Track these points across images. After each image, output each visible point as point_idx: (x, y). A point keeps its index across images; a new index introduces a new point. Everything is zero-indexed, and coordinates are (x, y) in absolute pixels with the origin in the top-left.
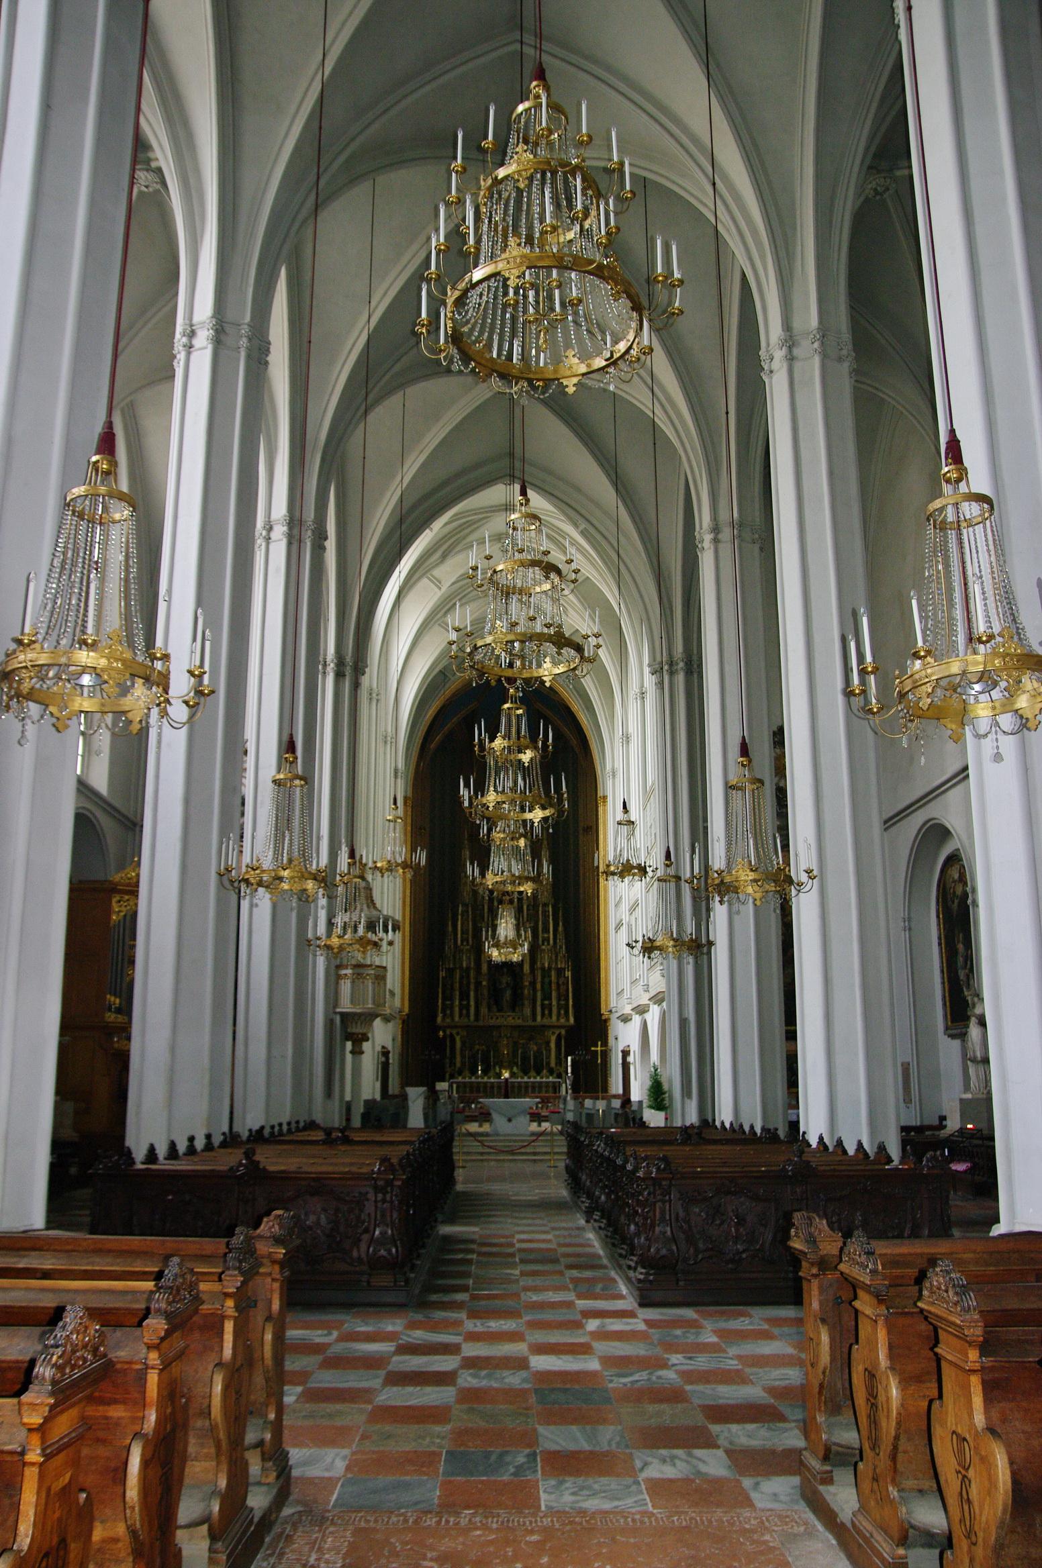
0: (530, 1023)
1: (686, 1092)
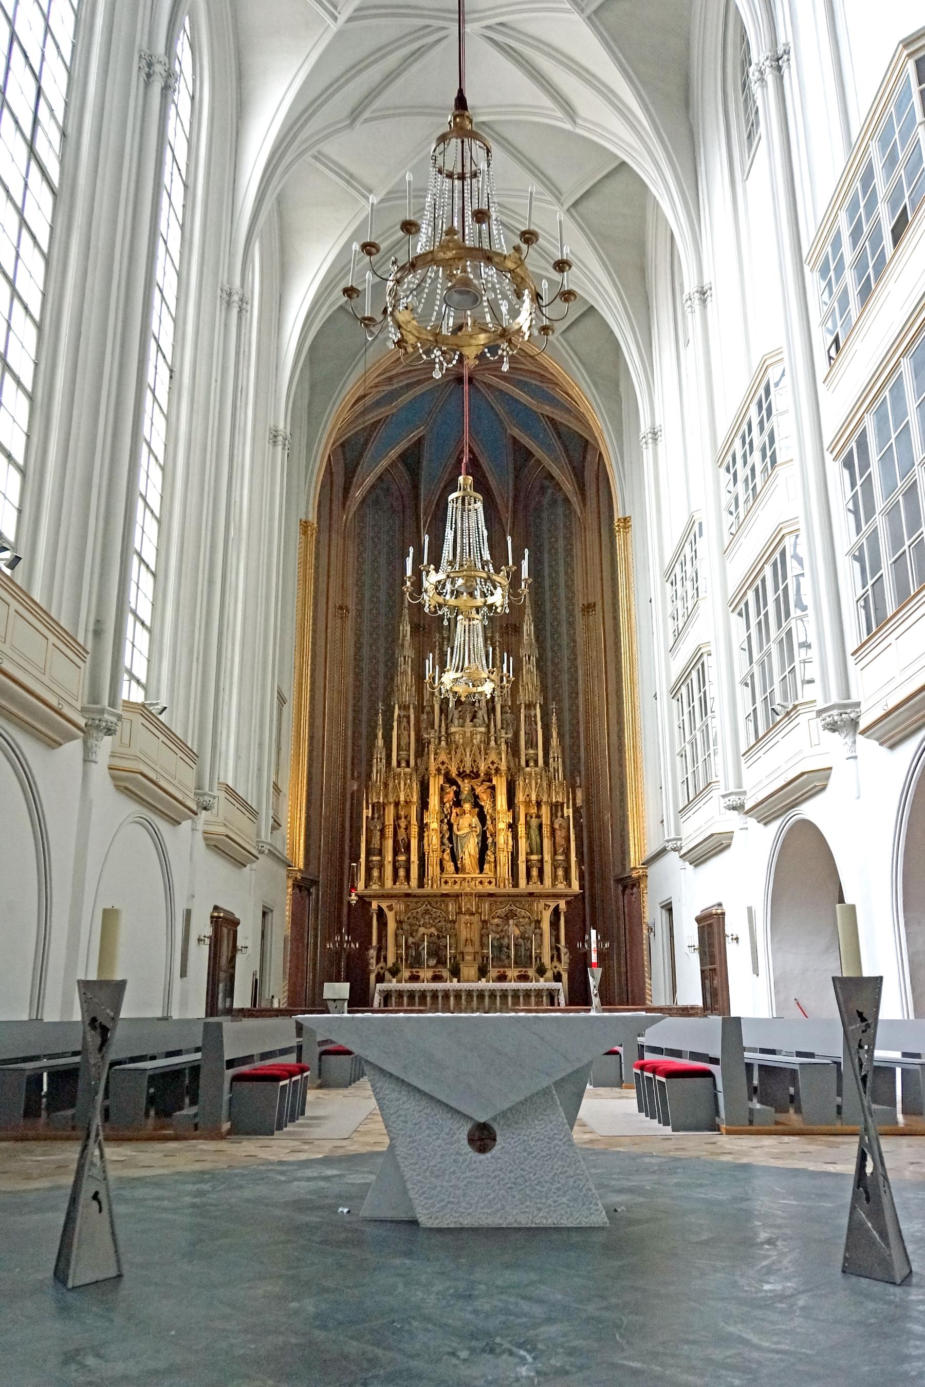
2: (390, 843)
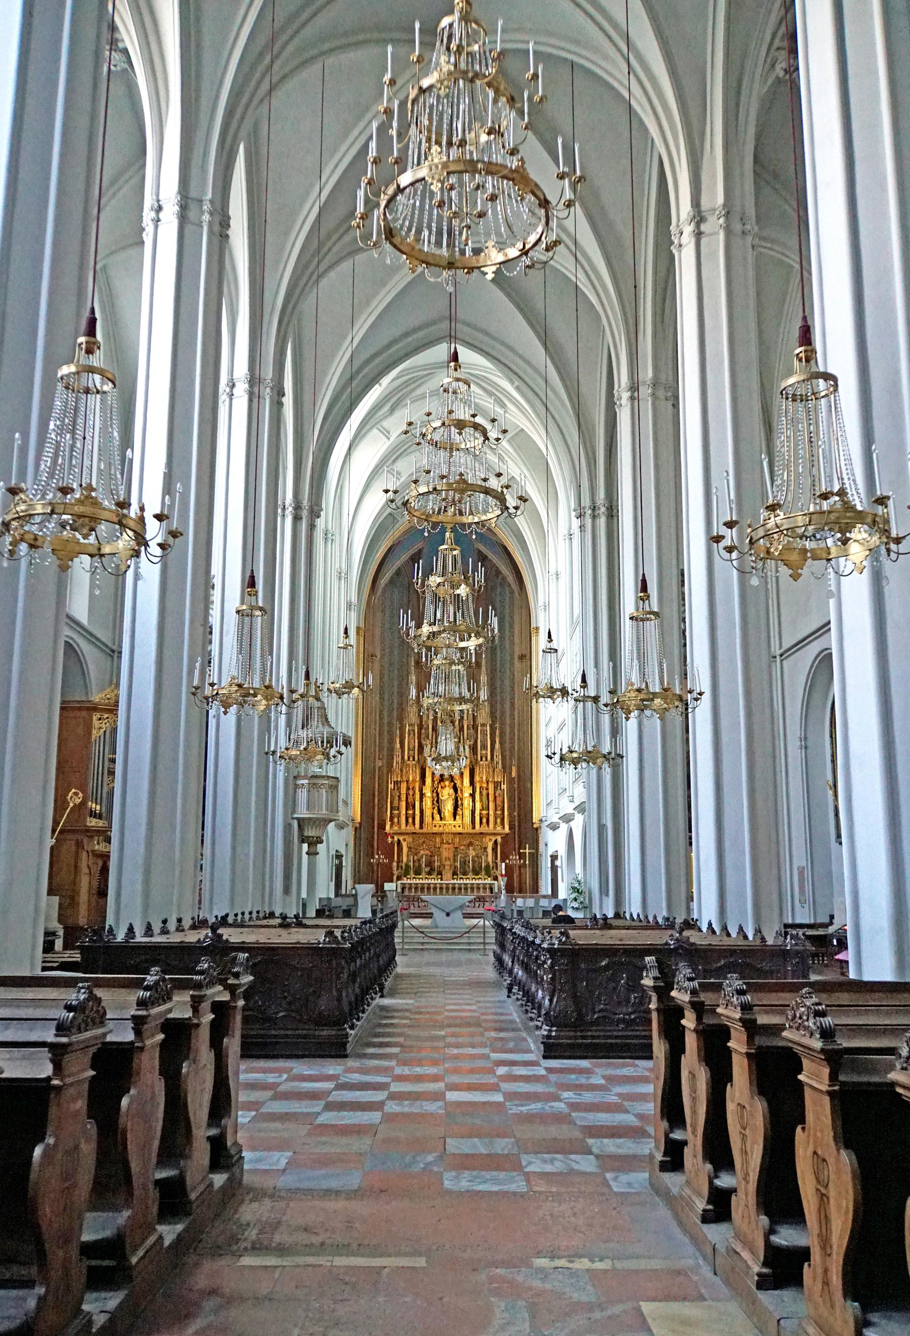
0: (470, 830)
1: (604, 891)
2: (404, 804)
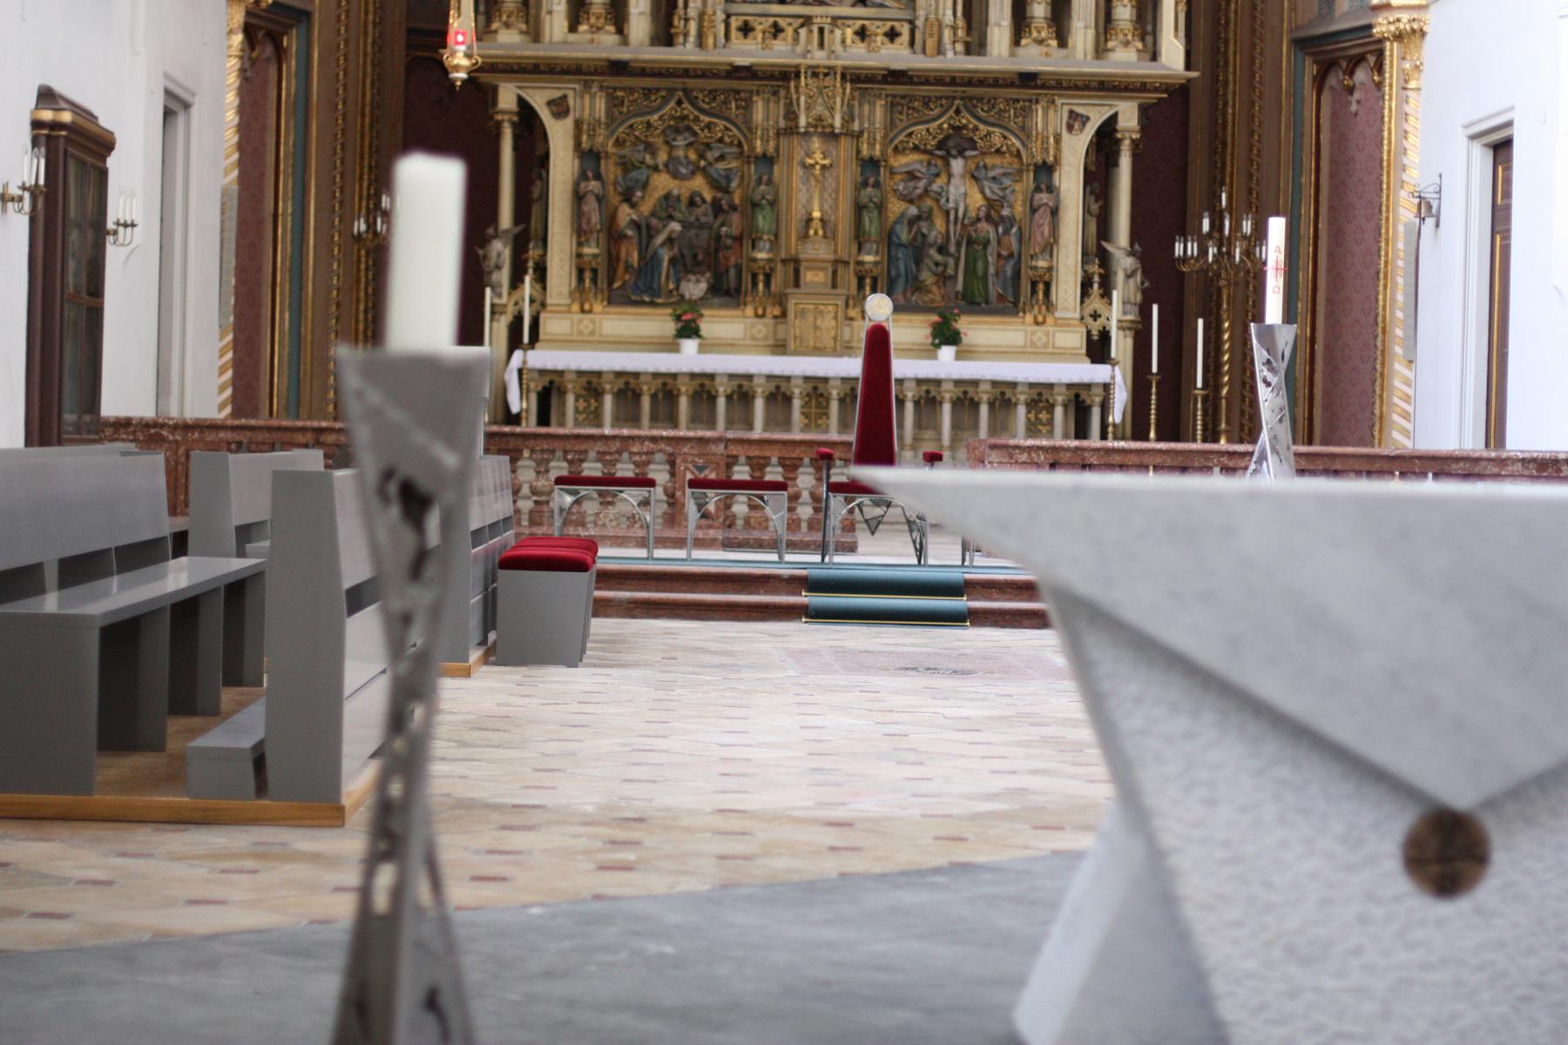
0: (954, 60)
